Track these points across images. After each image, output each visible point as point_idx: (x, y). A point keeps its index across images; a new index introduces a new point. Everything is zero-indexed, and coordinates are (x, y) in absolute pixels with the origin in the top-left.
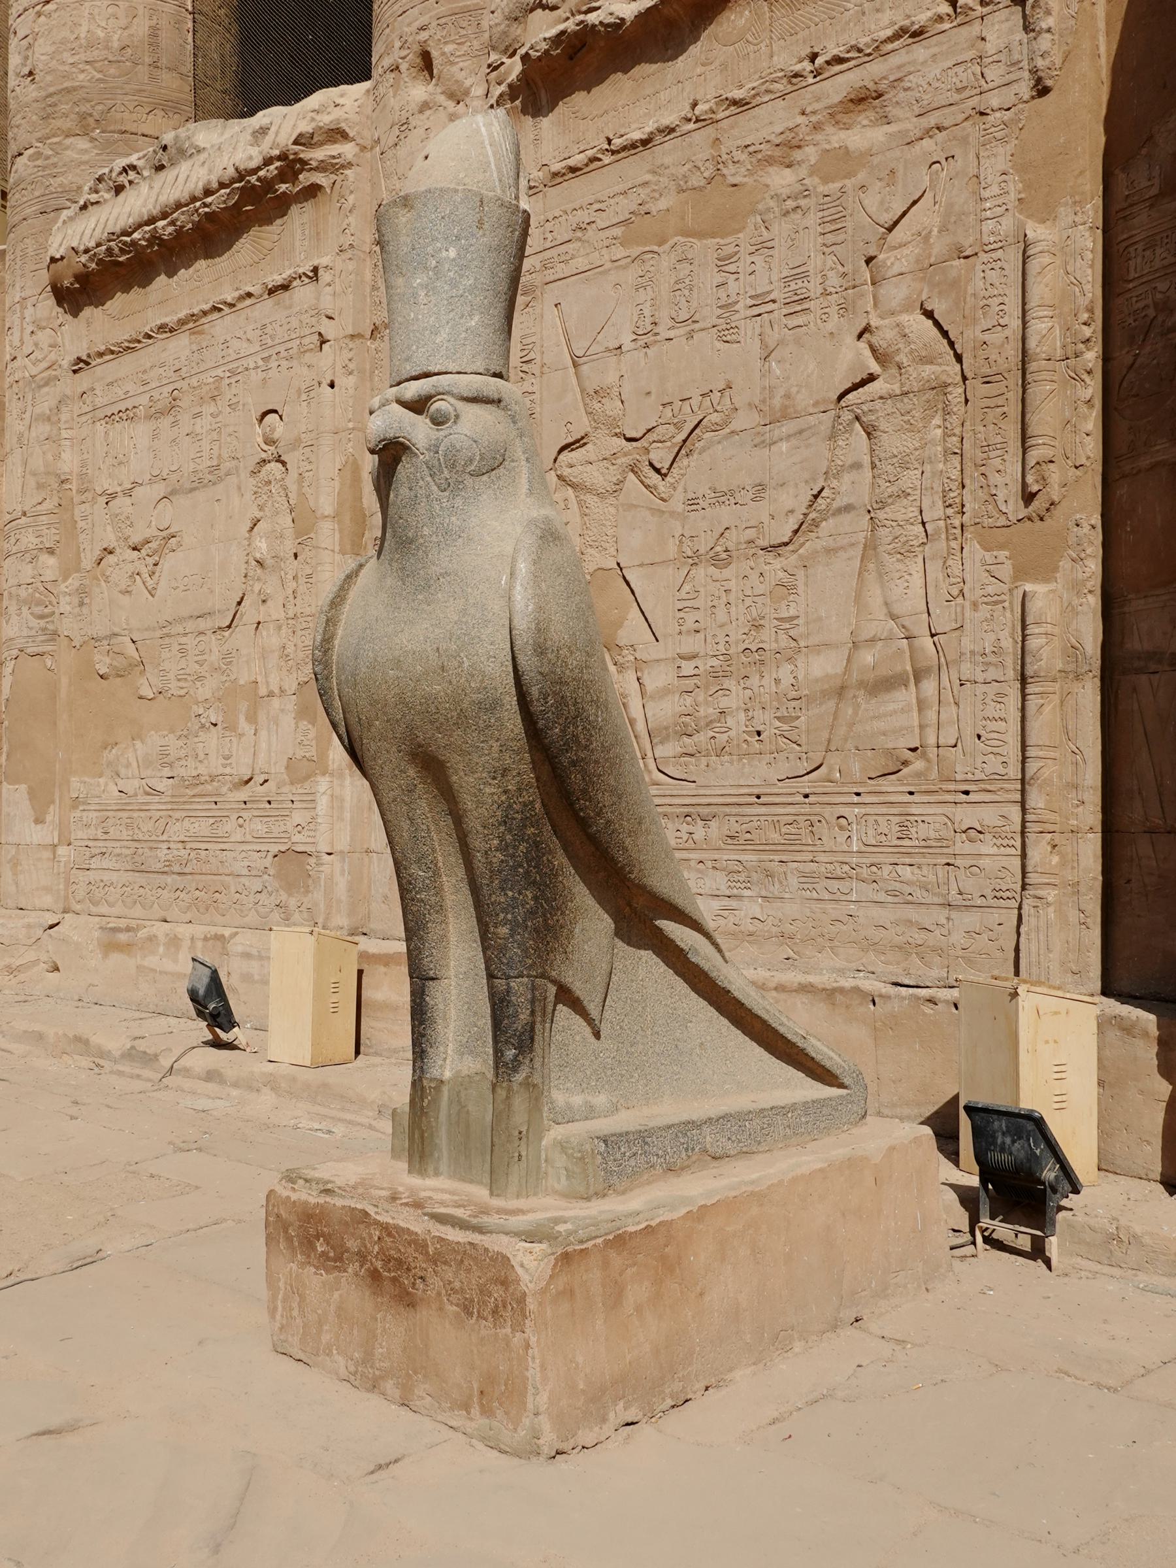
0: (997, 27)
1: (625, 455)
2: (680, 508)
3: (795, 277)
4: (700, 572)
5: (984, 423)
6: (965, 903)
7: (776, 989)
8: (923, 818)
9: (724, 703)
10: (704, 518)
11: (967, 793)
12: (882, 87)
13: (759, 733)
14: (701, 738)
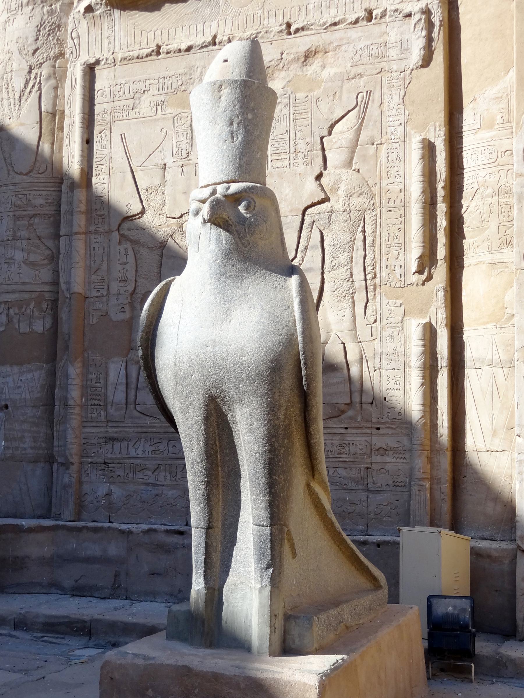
0: (396, 29)
5: (388, 232)
6: (377, 489)
8: (353, 442)
11: (378, 429)
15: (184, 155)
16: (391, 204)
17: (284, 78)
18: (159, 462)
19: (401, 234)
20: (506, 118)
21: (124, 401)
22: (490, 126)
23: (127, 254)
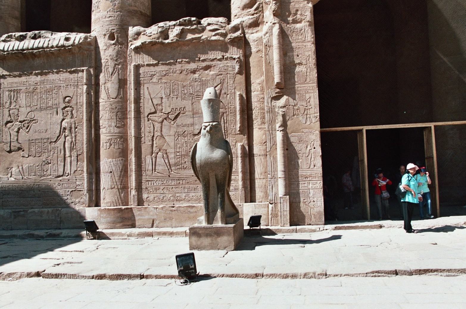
3: (197, 92)
10: (181, 129)
15: (168, 95)
16: (231, 111)
17: (199, 74)
18: (164, 187)
19: (234, 120)
20: (262, 89)
21: (152, 169)
22: (258, 91)
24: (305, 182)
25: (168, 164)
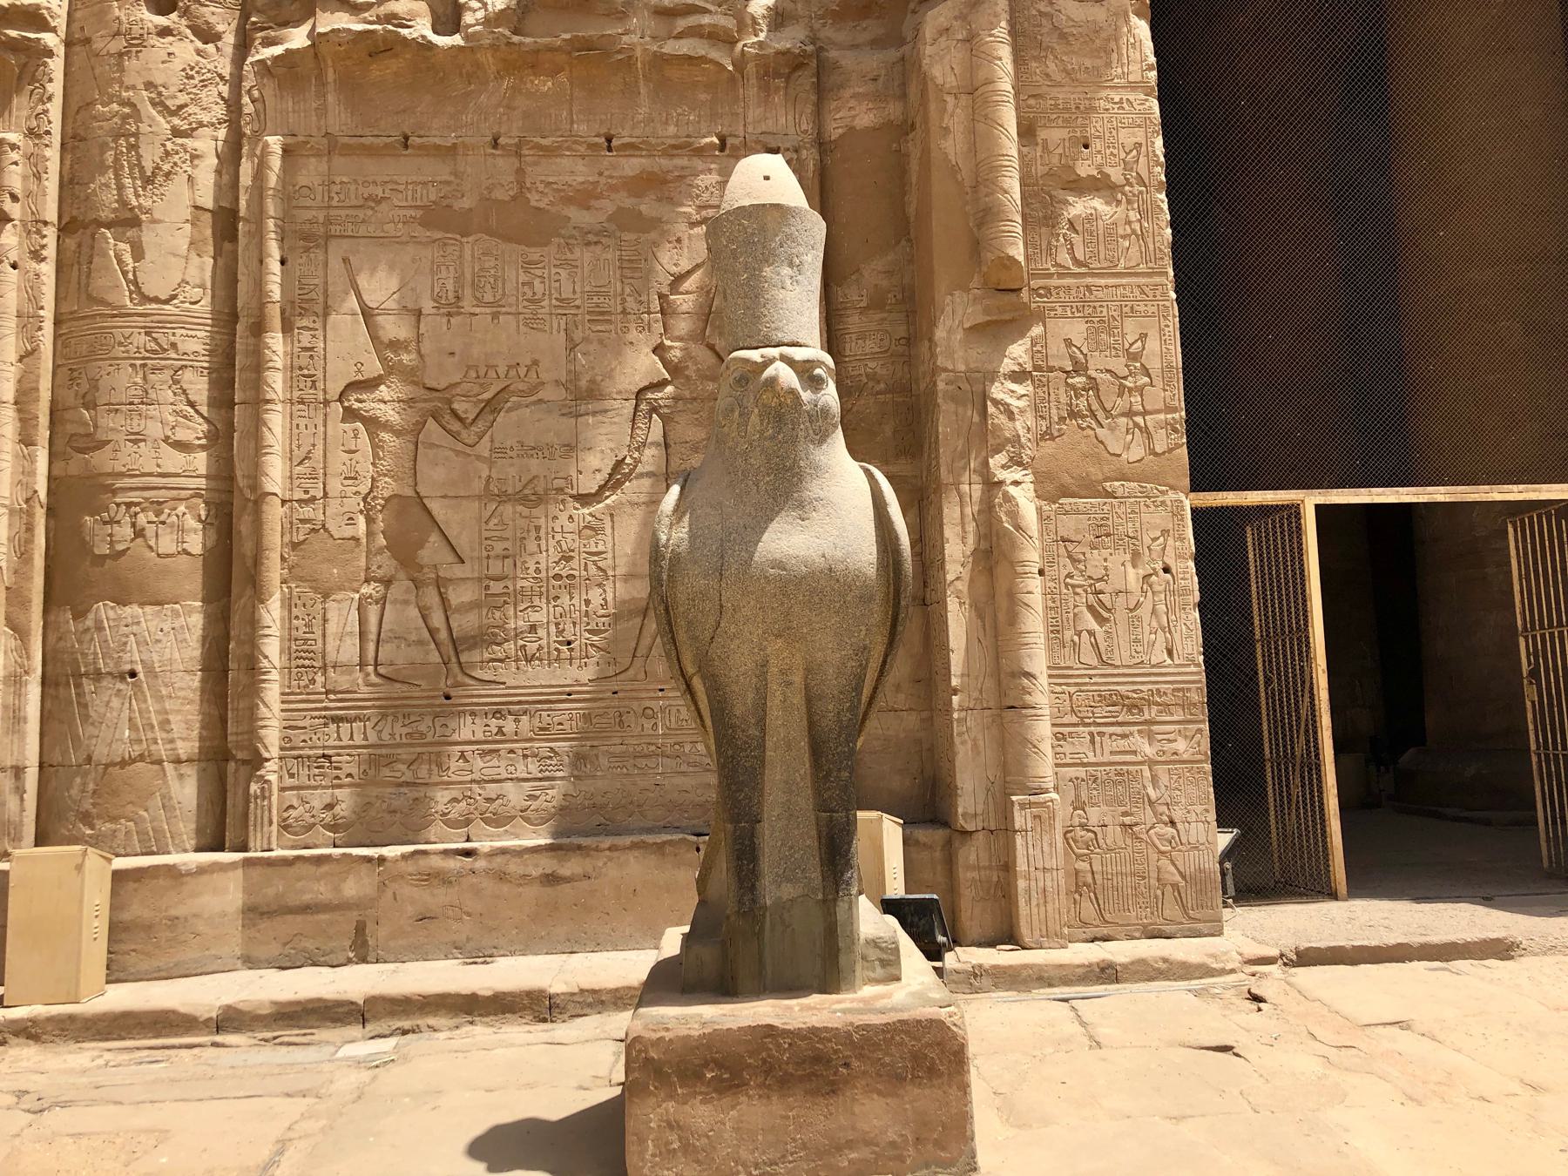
1: (425, 401)
2: (487, 454)
3: (598, 294)
4: (508, 509)
7: (609, 849)
9: (535, 617)
12: (669, 177)
13: (569, 643)
14: (510, 647)
18: (419, 750)
20: (899, 297)
21: (357, 660)
23: (356, 437)
24: (1126, 729)
25: (443, 635)
